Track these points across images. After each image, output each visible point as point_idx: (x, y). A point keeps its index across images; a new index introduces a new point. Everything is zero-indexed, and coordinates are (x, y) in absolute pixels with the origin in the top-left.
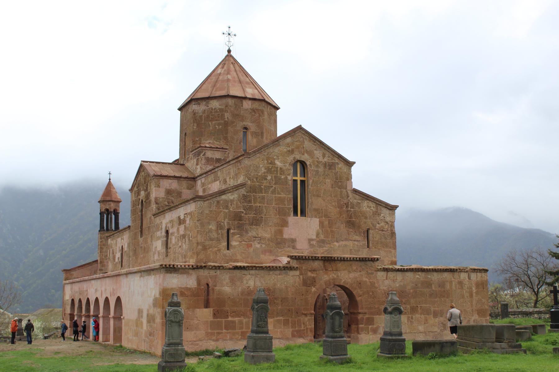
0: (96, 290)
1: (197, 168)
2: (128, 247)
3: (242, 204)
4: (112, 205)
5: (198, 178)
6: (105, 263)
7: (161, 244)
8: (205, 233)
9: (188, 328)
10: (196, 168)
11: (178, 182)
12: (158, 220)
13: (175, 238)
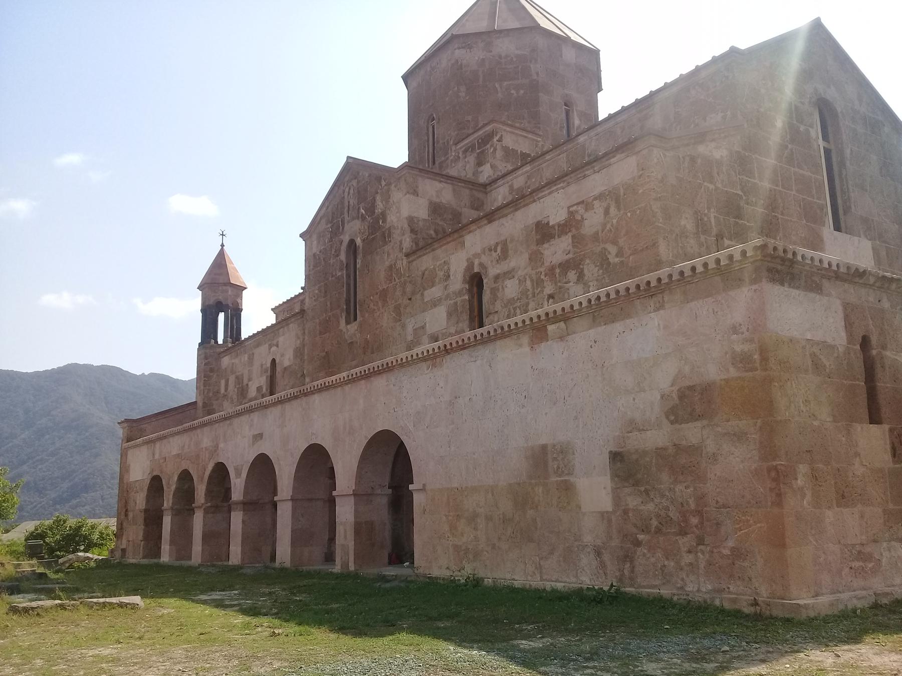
0: (259, 437)
1: (482, 172)
2: (295, 357)
3: (738, 176)
4: (230, 293)
5: (500, 182)
6: (214, 407)
7: (445, 315)
8: (674, 235)
9: (843, 497)
10: (476, 173)
11: (454, 190)
12: (426, 262)
13: (522, 281)
